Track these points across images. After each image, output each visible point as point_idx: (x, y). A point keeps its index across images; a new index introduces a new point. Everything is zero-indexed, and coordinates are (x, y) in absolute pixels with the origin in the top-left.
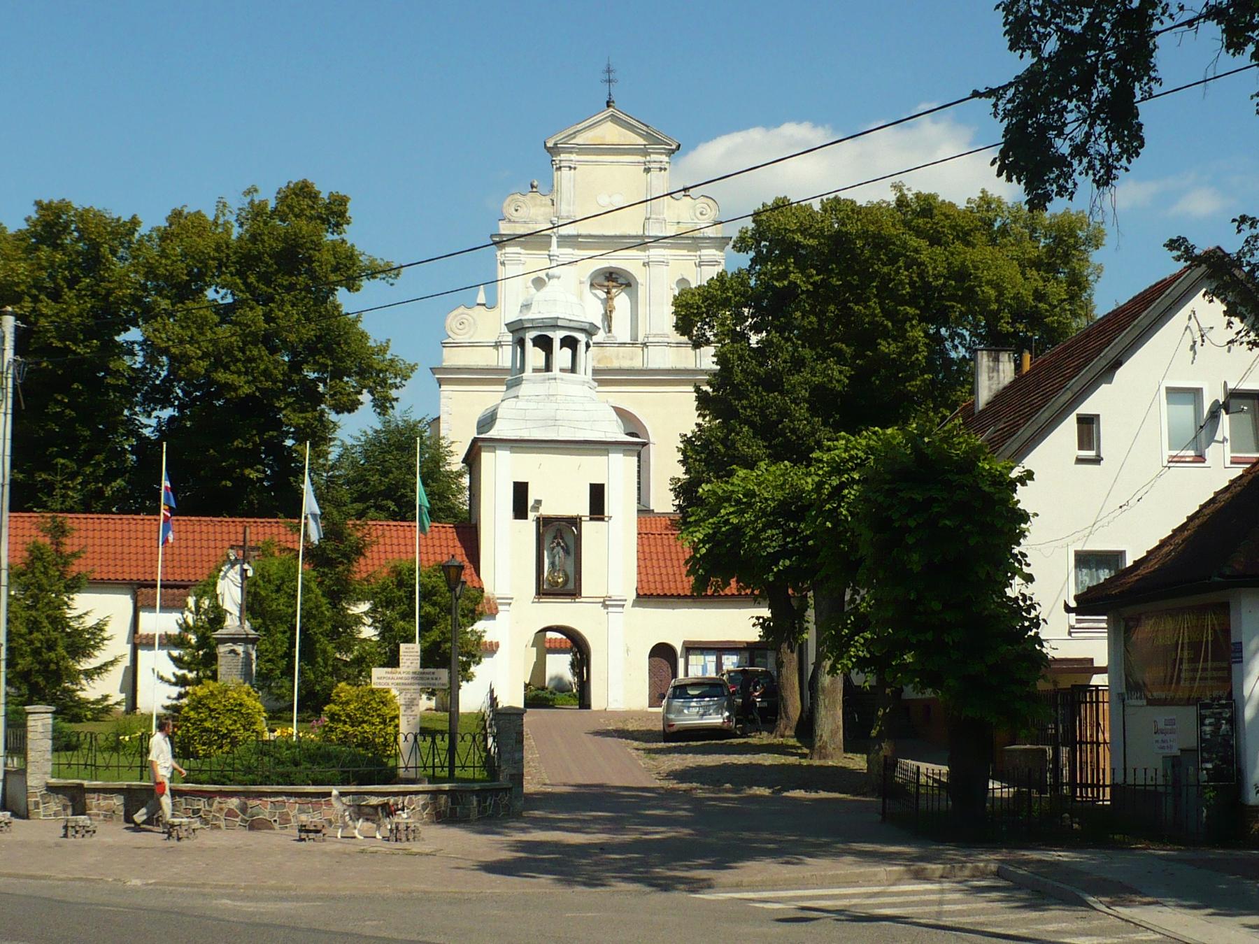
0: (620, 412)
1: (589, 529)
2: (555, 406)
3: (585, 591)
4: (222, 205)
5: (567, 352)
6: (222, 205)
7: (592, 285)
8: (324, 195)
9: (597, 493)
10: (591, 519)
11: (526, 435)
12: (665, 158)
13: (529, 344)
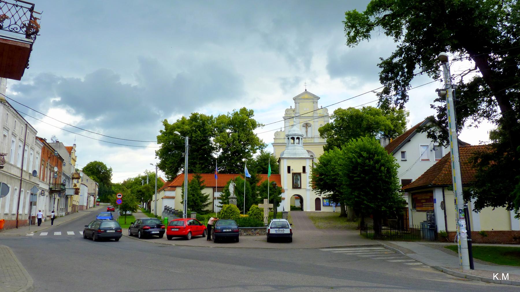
0: (308, 151)
1: (302, 175)
2: (295, 151)
4: (229, 113)
5: (298, 140)
6: (229, 113)
7: (303, 126)
8: (248, 110)
9: (304, 168)
11: (290, 157)
13: (290, 139)
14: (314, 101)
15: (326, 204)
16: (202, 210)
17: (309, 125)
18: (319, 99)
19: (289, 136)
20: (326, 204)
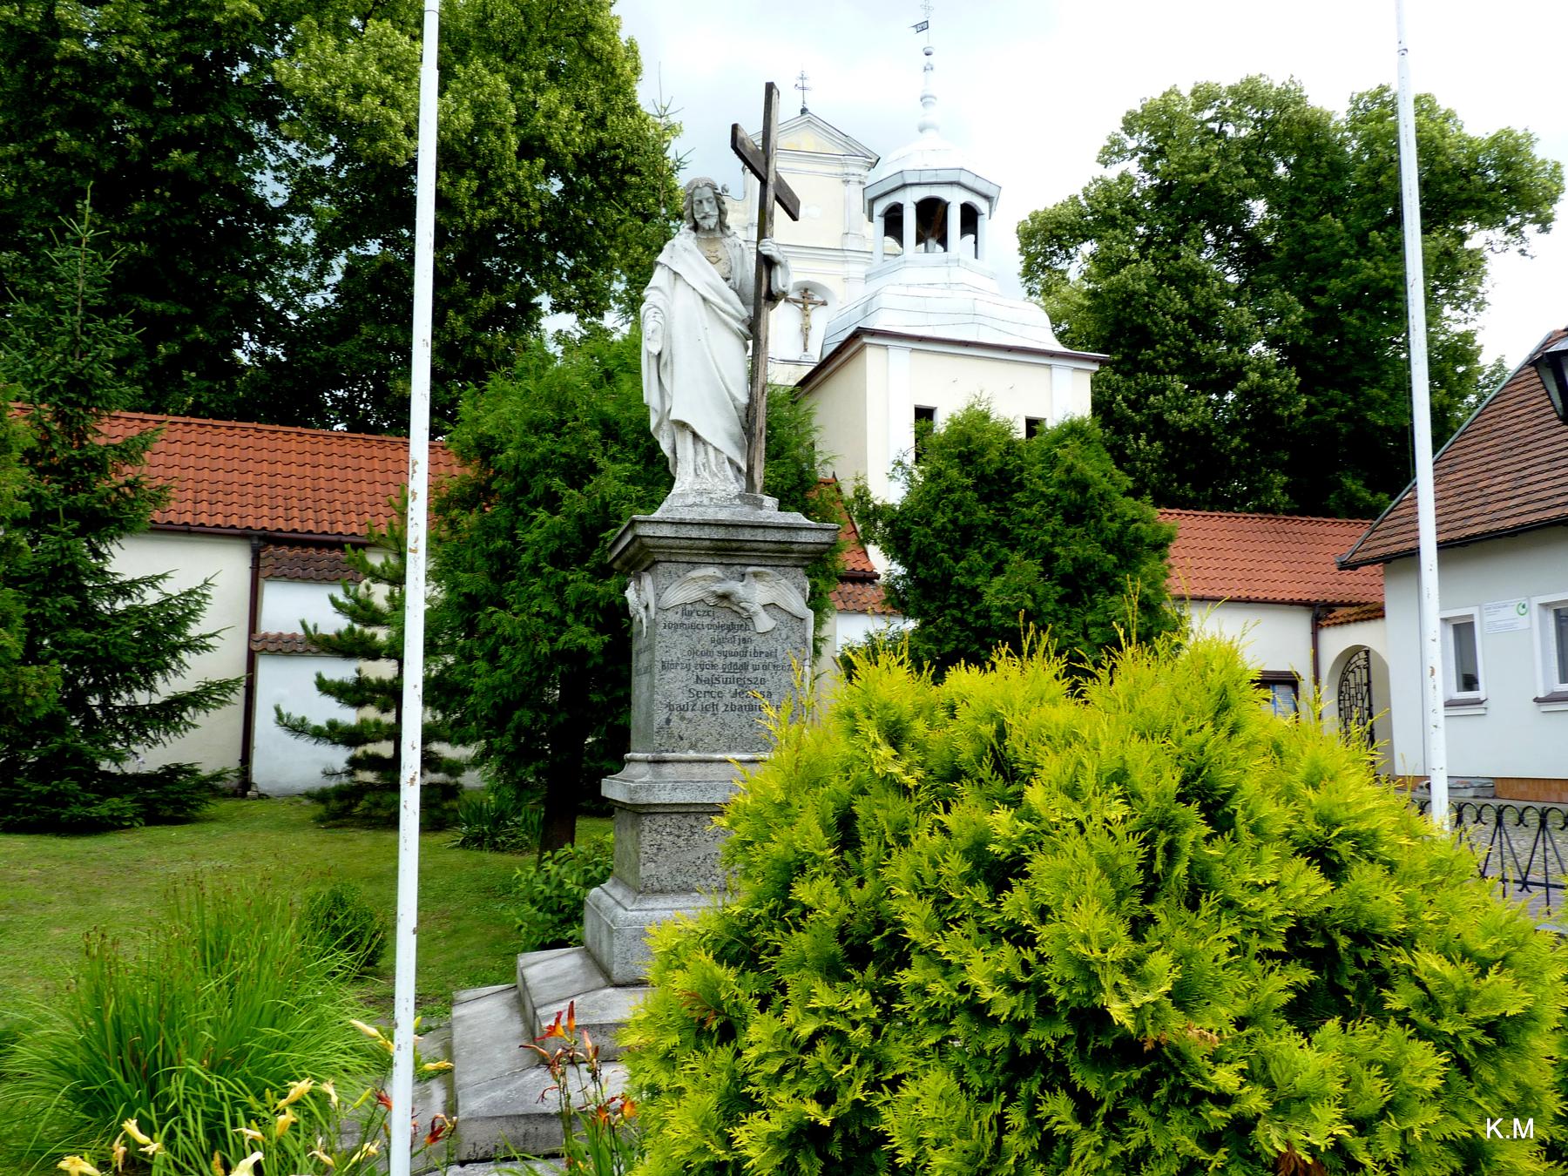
16: (105, 765)
17: (817, 298)
18: (874, 165)
19: (904, 186)
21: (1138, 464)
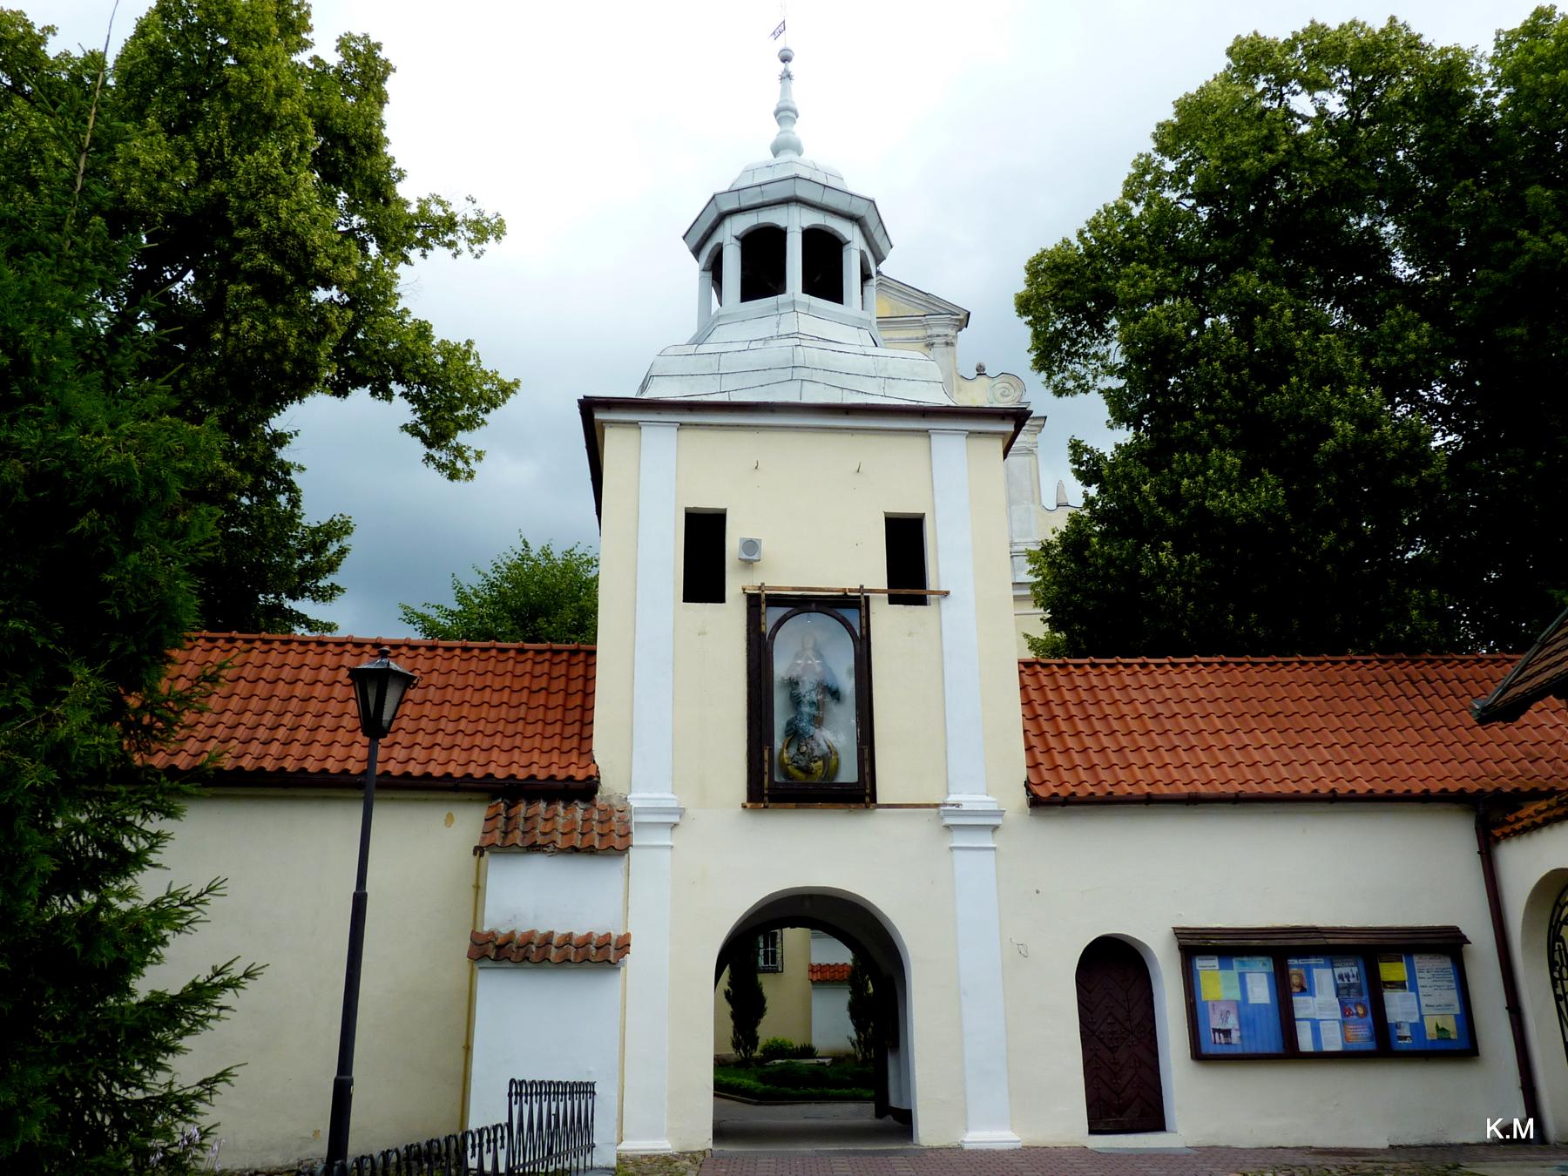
1: (887, 620)
3: (886, 790)
10: (893, 600)
12: (951, 332)
14: (929, 332)
15: (1232, 1023)
20: (1232, 1023)
21: (1162, 590)
